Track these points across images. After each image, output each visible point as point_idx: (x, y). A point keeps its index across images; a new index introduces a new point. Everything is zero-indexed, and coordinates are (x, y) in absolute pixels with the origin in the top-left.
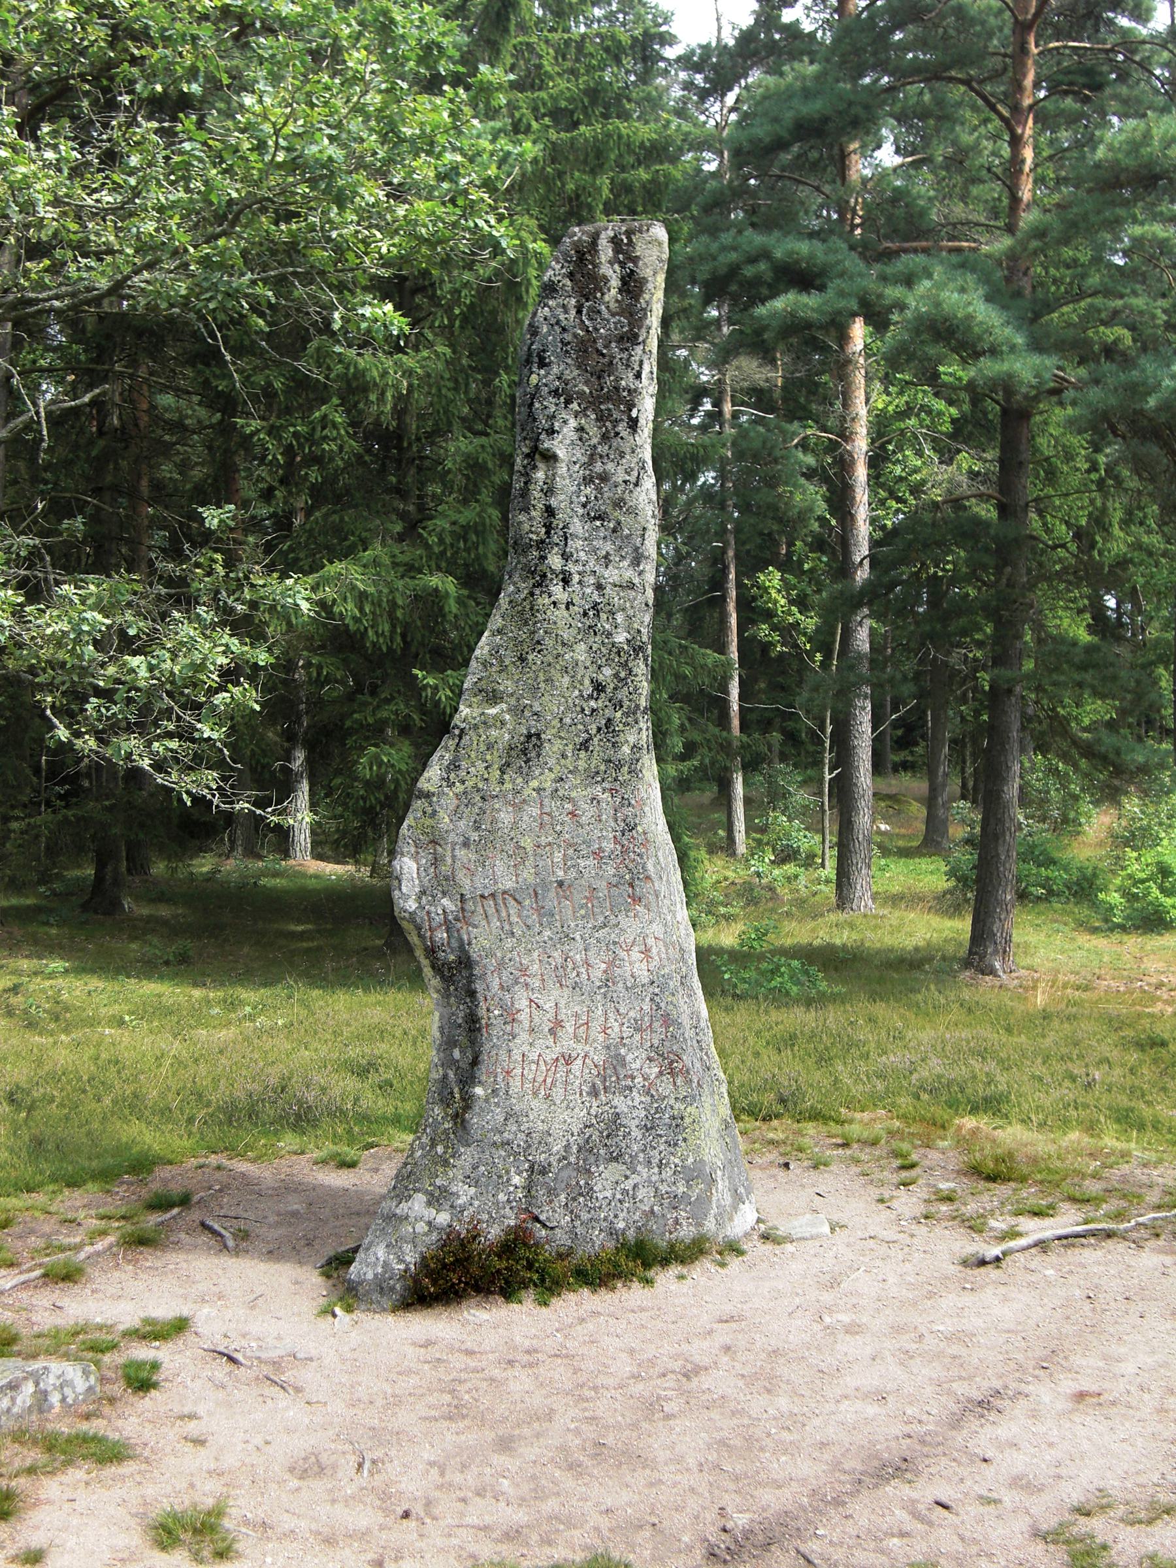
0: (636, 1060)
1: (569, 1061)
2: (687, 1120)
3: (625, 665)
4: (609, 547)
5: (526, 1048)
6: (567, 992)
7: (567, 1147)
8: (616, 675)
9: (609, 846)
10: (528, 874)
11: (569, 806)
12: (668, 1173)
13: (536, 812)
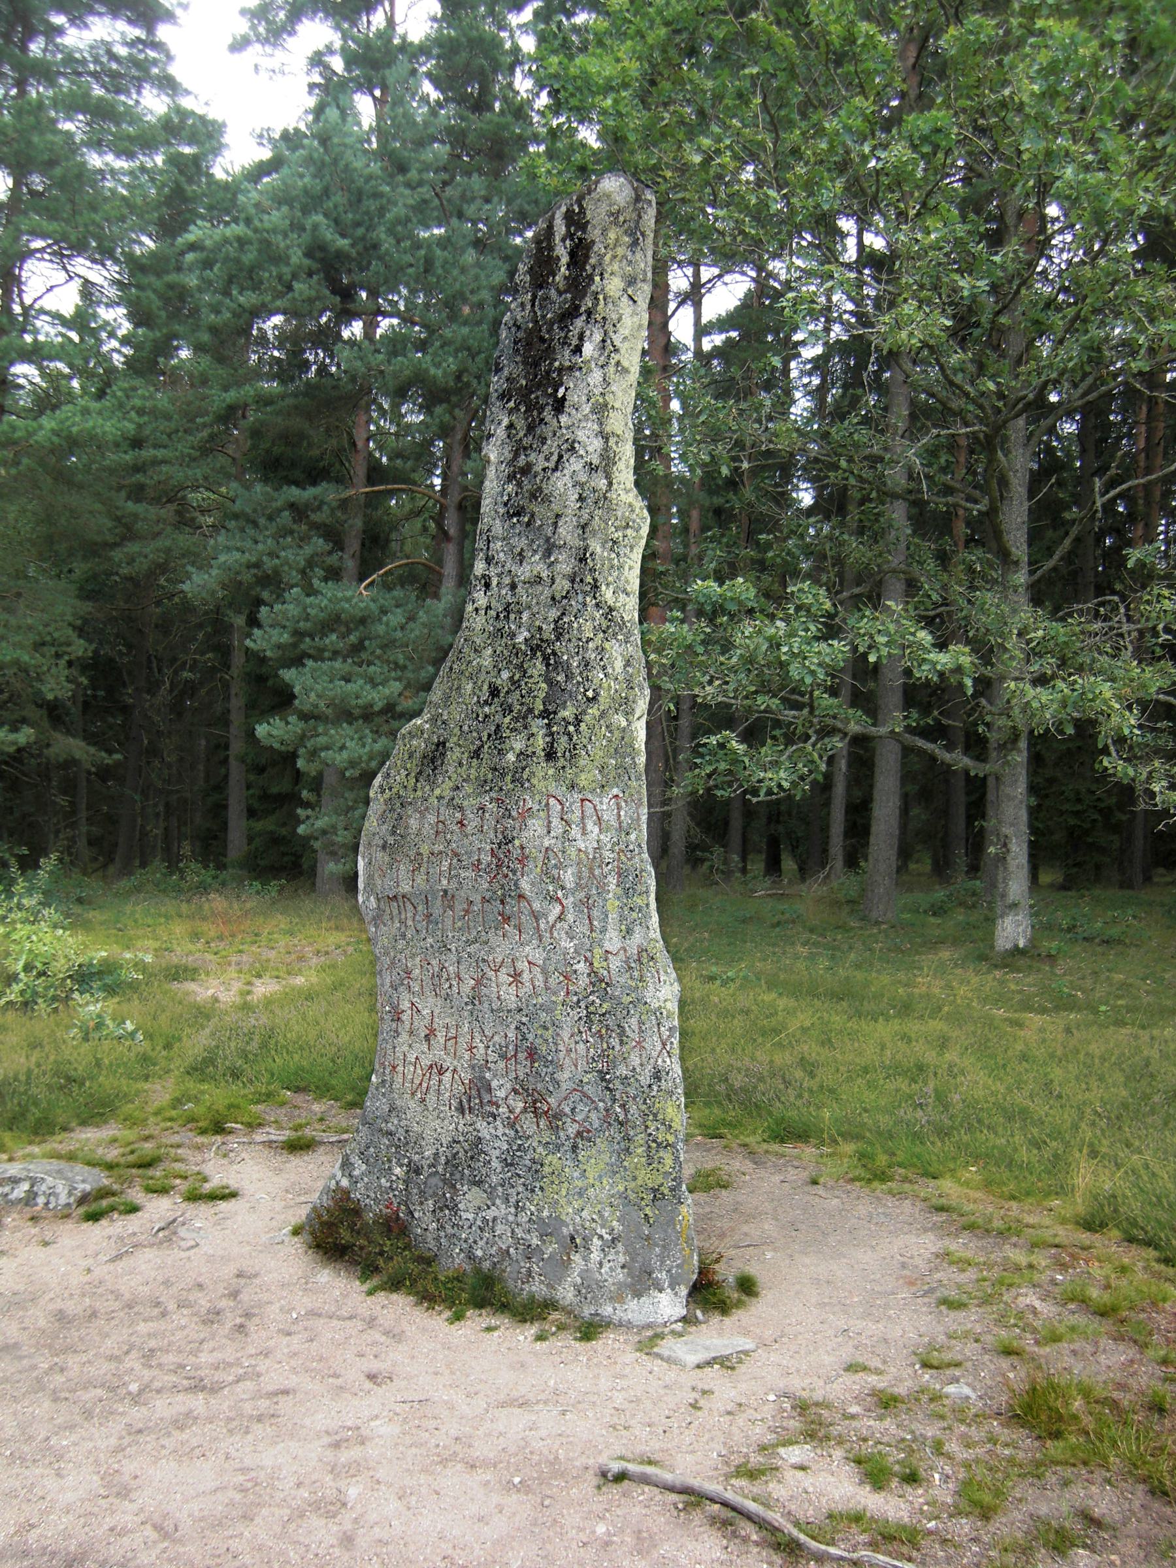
0: (501, 1088)
2: (547, 1170)
3: (520, 667)
4: (523, 542)
5: (405, 1048)
6: (440, 1002)
7: (436, 1155)
8: (511, 678)
9: (486, 858)
10: (420, 879)
11: (458, 815)
12: (523, 1218)
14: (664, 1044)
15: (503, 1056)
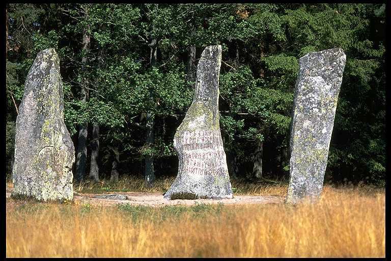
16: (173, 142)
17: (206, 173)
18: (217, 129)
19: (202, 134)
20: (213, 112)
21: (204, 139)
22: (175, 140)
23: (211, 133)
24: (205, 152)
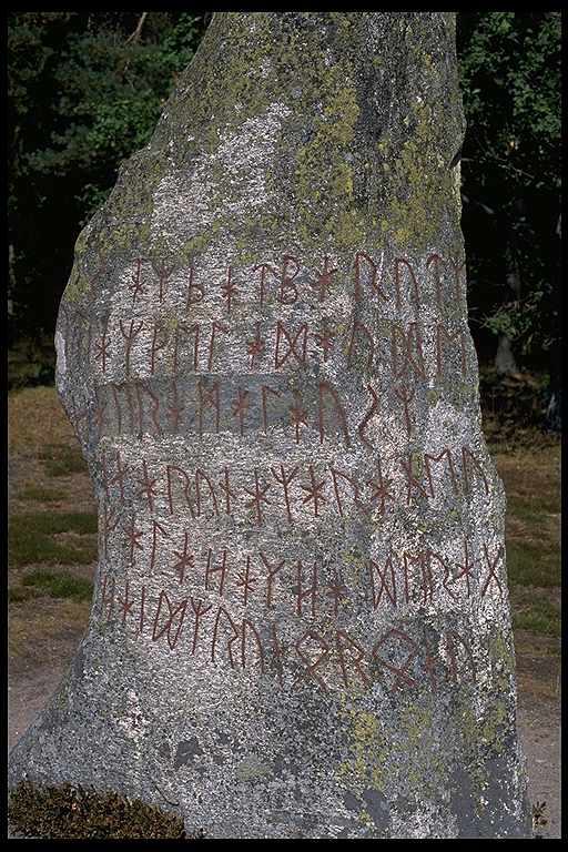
1: (199, 611)
13: (184, 283)
14: (492, 570)
15: (296, 591)
16: (52, 351)
17: (273, 658)
18: (418, 240)
19: (248, 295)
20: (367, 81)
21: (271, 336)
22: (60, 341)
23: (325, 281)
24: (271, 462)
